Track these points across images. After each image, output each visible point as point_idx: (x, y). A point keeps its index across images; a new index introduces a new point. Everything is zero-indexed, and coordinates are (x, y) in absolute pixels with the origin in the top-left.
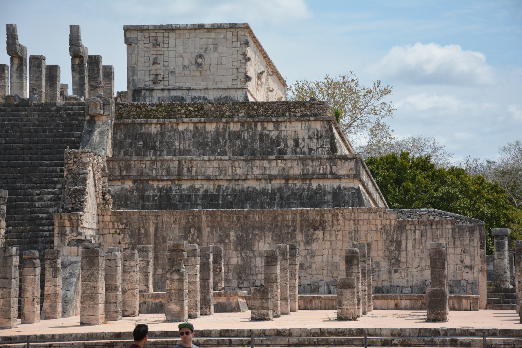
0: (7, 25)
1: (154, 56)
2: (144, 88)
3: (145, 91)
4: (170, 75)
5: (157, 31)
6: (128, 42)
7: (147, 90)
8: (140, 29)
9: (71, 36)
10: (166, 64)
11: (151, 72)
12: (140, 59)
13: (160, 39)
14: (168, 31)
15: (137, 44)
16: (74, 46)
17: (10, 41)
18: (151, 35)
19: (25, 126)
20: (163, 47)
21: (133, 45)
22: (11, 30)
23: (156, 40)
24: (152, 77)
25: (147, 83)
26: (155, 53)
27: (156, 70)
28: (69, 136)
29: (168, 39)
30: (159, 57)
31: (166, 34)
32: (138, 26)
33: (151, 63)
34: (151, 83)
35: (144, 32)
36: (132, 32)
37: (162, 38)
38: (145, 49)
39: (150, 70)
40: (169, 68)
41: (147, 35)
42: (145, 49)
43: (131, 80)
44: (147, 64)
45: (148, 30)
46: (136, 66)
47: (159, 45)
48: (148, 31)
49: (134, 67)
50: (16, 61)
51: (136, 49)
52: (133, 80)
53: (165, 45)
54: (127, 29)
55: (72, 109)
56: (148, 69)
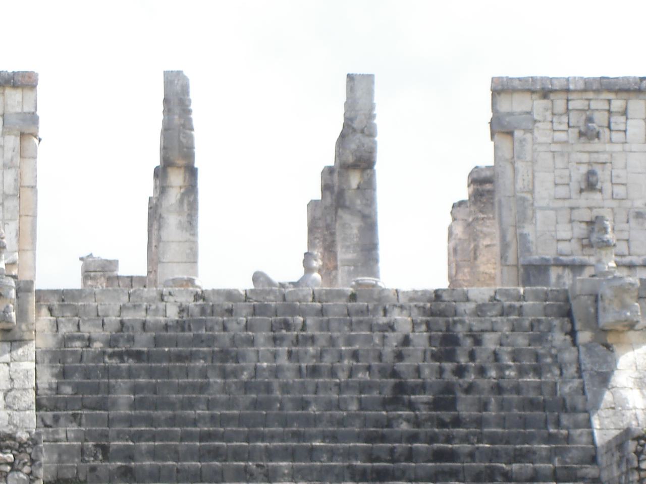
0: (167, 74)
1: (584, 169)
2: (556, 260)
3: (559, 270)
4: (633, 222)
5: (591, 95)
6: (501, 128)
7: (565, 266)
8: (544, 90)
9: (351, 105)
10: (620, 191)
11: (577, 214)
12: (540, 176)
13: (600, 118)
14: (625, 95)
15: (531, 131)
16: (359, 135)
17: (177, 120)
18: (572, 105)
19: (399, 356)
20: (611, 141)
21: (518, 134)
22: (178, 88)
23: (590, 120)
24: (580, 230)
25: (564, 247)
26: (585, 158)
27: (590, 208)
28: (539, 388)
29: (623, 119)
30: (598, 169)
31: (617, 104)
32: (533, 79)
33: (575, 186)
34: (575, 246)
35: (552, 96)
36: (517, 97)
37: (606, 114)
38: (555, 148)
39: (572, 209)
40: (628, 204)
41: (560, 104)
42: (555, 148)
43: (510, 237)
44: (562, 191)
45: (568, 91)
46: (529, 196)
47: (598, 135)
48: (563, 96)
49: (524, 200)
50: (176, 178)
51: (528, 147)
52: (523, 236)
53: (616, 136)
54: (501, 89)
55: (520, 311)
56: (567, 204)
